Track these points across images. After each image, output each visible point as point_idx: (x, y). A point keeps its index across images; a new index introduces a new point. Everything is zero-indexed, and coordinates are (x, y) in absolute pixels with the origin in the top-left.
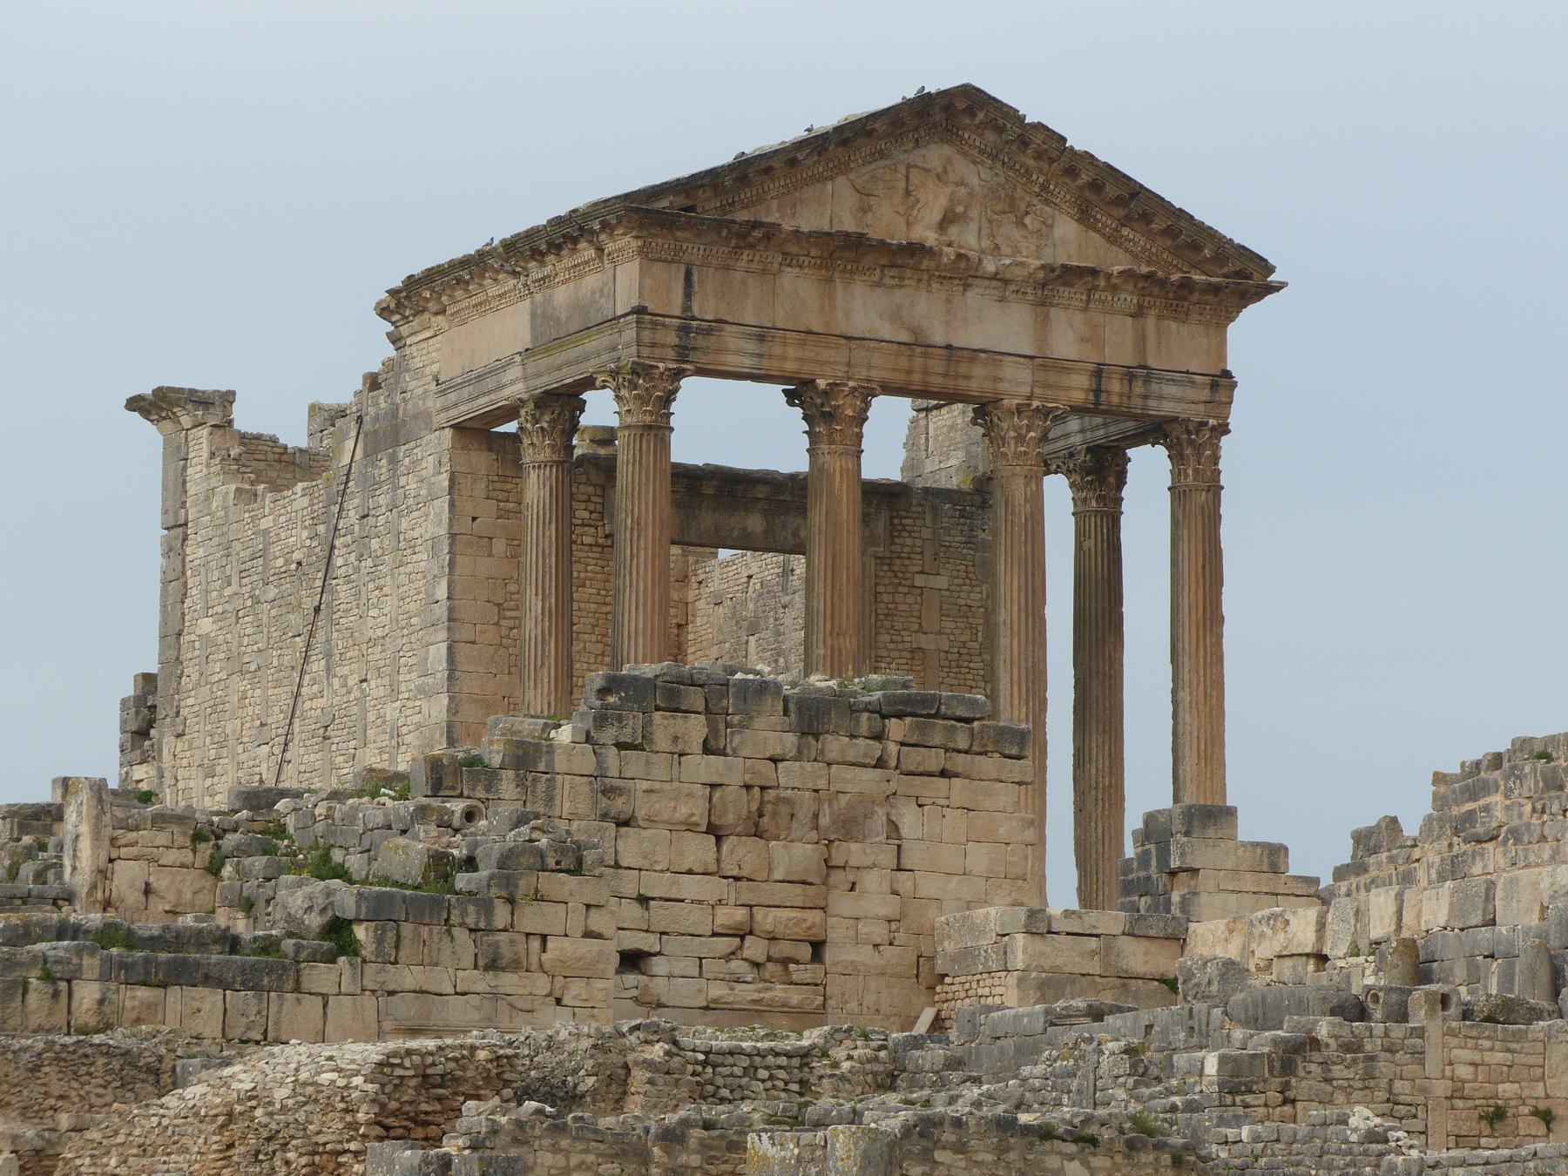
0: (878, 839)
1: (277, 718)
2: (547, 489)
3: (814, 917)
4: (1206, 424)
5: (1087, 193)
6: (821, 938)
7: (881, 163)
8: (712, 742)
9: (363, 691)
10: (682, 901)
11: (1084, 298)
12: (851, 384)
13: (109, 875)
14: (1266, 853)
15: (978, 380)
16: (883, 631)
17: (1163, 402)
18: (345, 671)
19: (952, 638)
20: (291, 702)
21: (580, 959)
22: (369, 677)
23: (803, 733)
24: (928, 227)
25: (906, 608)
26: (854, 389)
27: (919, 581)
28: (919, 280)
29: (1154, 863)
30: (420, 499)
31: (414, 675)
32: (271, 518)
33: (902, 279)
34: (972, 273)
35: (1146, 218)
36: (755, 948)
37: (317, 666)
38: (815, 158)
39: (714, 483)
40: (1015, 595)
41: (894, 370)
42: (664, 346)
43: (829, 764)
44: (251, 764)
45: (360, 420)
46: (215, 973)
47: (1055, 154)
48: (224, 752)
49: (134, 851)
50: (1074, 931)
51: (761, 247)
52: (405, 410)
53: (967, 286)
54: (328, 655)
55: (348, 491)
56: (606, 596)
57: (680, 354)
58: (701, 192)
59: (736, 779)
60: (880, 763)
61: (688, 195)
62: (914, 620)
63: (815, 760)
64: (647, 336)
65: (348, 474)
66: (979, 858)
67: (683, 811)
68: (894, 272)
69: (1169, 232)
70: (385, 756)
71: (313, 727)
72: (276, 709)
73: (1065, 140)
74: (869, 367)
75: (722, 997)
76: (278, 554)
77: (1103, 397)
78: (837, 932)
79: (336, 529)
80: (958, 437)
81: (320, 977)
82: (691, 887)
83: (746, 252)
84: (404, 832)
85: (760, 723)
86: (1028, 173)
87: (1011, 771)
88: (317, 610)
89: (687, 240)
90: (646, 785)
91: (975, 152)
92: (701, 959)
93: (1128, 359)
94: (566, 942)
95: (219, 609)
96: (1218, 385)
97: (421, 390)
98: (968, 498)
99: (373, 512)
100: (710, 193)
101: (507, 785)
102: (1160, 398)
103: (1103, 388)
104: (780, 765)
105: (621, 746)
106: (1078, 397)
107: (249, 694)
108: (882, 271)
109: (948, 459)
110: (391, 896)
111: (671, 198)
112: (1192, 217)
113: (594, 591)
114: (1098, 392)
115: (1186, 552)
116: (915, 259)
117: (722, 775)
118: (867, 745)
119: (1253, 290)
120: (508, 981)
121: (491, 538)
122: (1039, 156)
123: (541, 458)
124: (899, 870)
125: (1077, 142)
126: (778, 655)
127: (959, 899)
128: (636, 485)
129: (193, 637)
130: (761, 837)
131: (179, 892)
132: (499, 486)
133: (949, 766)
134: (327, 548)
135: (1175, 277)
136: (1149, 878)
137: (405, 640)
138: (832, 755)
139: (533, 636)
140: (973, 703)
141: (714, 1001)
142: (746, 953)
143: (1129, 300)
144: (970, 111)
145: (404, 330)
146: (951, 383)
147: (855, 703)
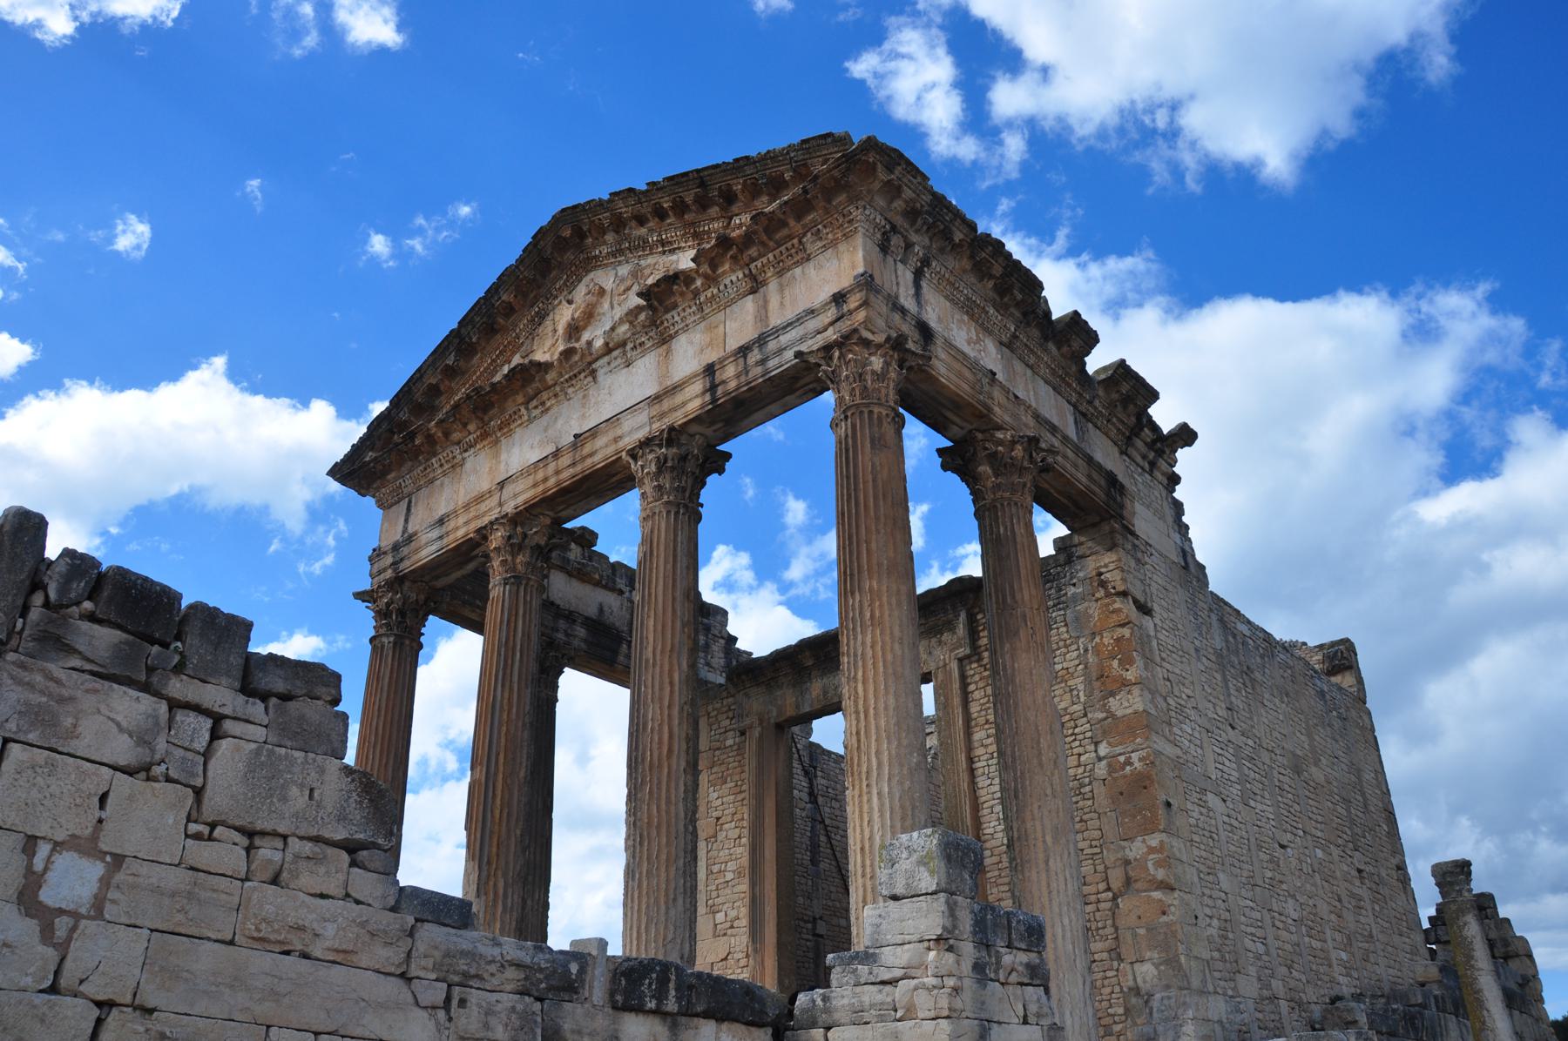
11: (694, 308)
15: (601, 452)
16: (977, 729)
28: (556, 395)
33: (543, 404)
34: (589, 359)
35: (729, 198)
41: (535, 485)
42: (385, 570)
53: (593, 373)
56: (741, 785)
57: (394, 570)
68: (534, 403)
69: (754, 191)
73: (631, 190)
74: (515, 496)
77: (720, 391)
83: (434, 460)
86: (645, 241)
89: (396, 479)
96: (844, 295)
102: (780, 351)
103: (717, 381)
108: (527, 409)
111: (370, 454)
112: (747, 158)
113: (733, 784)
114: (713, 388)
122: (641, 221)
143: (734, 278)
144: (580, 235)
146: (579, 468)
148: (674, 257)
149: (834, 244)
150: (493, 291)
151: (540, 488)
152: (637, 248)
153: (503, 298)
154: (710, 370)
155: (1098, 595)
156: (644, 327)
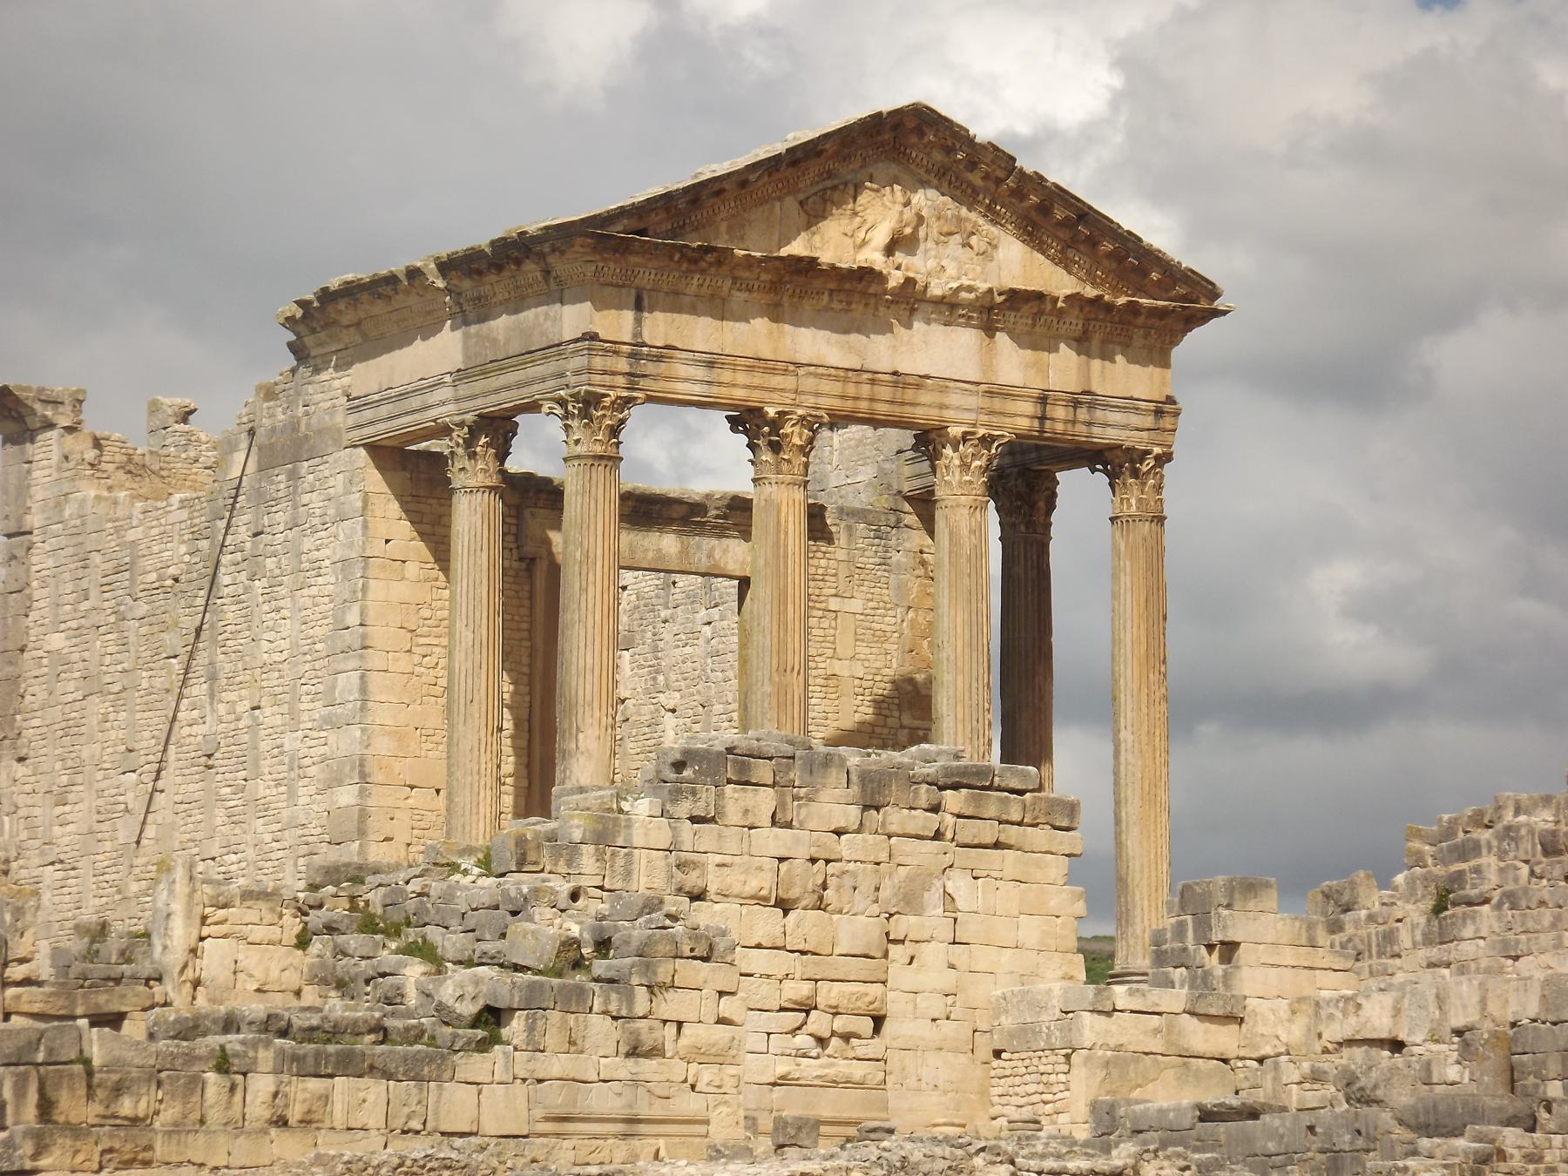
0: (934, 913)
1: (147, 742)
2: (479, 515)
3: (876, 989)
4: (1149, 452)
5: (1034, 215)
6: (882, 1013)
7: (829, 183)
8: (778, 816)
9: (255, 718)
10: (752, 975)
11: (1030, 322)
12: (800, 412)
13: (199, 953)
14: (1304, 926)
15: (925, 410)
17: (1108, 429)
18: (232, 696)
19: (867, 664)
20: (166, 727)
21: (714, 1045)
22: (262, 704)
23: (866, 808)
24: (875, 250)
25: (821, 632)
26: (803, 418)
27: (834, 604)
28: (866, 305)
29: (1190, 934)
30: (327, 519)
31: (318, 704)
32: (139, 529)
33: (849, 303)
36: (819, 1022)
37: (198, 689)
38: (766, 179)
39: (630, 503)
40: (959, 630)
41: (842, 397)
42: (614, 373)
43: (890, 837)
44: (114, 791)
45: (252, 433)
46: (379, 1063)
47: (1000, 174)
48: (79, 778)
49: (224, 929)
50: (1138, 1008)
51: (713, 270)
52: (308, 425)
53: (913, 311)
54: (212, 678)
55: (238, 506)
58: (653, 215)
59: (803, 852)
60: (938, 836)
61: (641, 218)
62: (828, 645)
63: (876, 832)
64: (598, 362)
65: (238, 488)
66: (1030, 930)
67: (753, 885)
68: (843, 296)
70: (283, 789)
71: (193, 754)
72: (147, 734)
74: (817, 394)
75: (789, 1073)
76: (149, 568)
77: (1048, 424)
78: (895, 1005)
79: (223, 546)
80: (870, 452)
81: (474, 1065)
82: (757, 961)
83: (697, 276)
84: (514, 913)
85: (825, 795)
87: (1061, 843)
88: (199, 631)
90: (719, 859)
91: (922, 171)
92: (769, 1034)
93: (1073, 387)
94: (700, 1028)
95: (74, 624)
96: (1163, 412)
97: (329, 404)
98: (883, 518)
99: (269, 530)
100: (663, 215)
101: (588, 859)
103: (1048, 415)
104: (843, 837)
105: (694, 820)
106: (1023, 424)
107: (111, 717)
108: (830, 295)
109: (856, 474)
110: (542, 985)
112: (1140, 240)
114: (1042, 418)
115: (1129, 585)
116: (863, 283)
117: (789, 849)
118: (926, 817)
119: (1199, 315)
120: (647, 1067)
121: (404, 562)
123: (473, 483)
124: (954, 943)
125: (1026, 163)
126: (657, 672)
127: (1012, 973)
128: (585, 516)
129: (40, 653)
130: (824, 910)
131: (267, 969)
132: (413, 506)
133: (1002, 839)
134: (211, 564)
135: (1122, 300)
136: (1185, 950)
137: (308, 666)
138: (893, 828)
139: (463, 668)
140: (1026, 775)
141: (782, 1078)
142: (810, 1028)
143: (1074, 322)
145: (309, 340)
146: (897, 410)
147: (914, 776)
148: (995, 231)
149: (1150, 349)
150: (826, 137)
151: (849, 404)
152: (956, 188)
153: (827, 146)
154: (1043, 400)
155: (917, 572)
156: (983, 307)
